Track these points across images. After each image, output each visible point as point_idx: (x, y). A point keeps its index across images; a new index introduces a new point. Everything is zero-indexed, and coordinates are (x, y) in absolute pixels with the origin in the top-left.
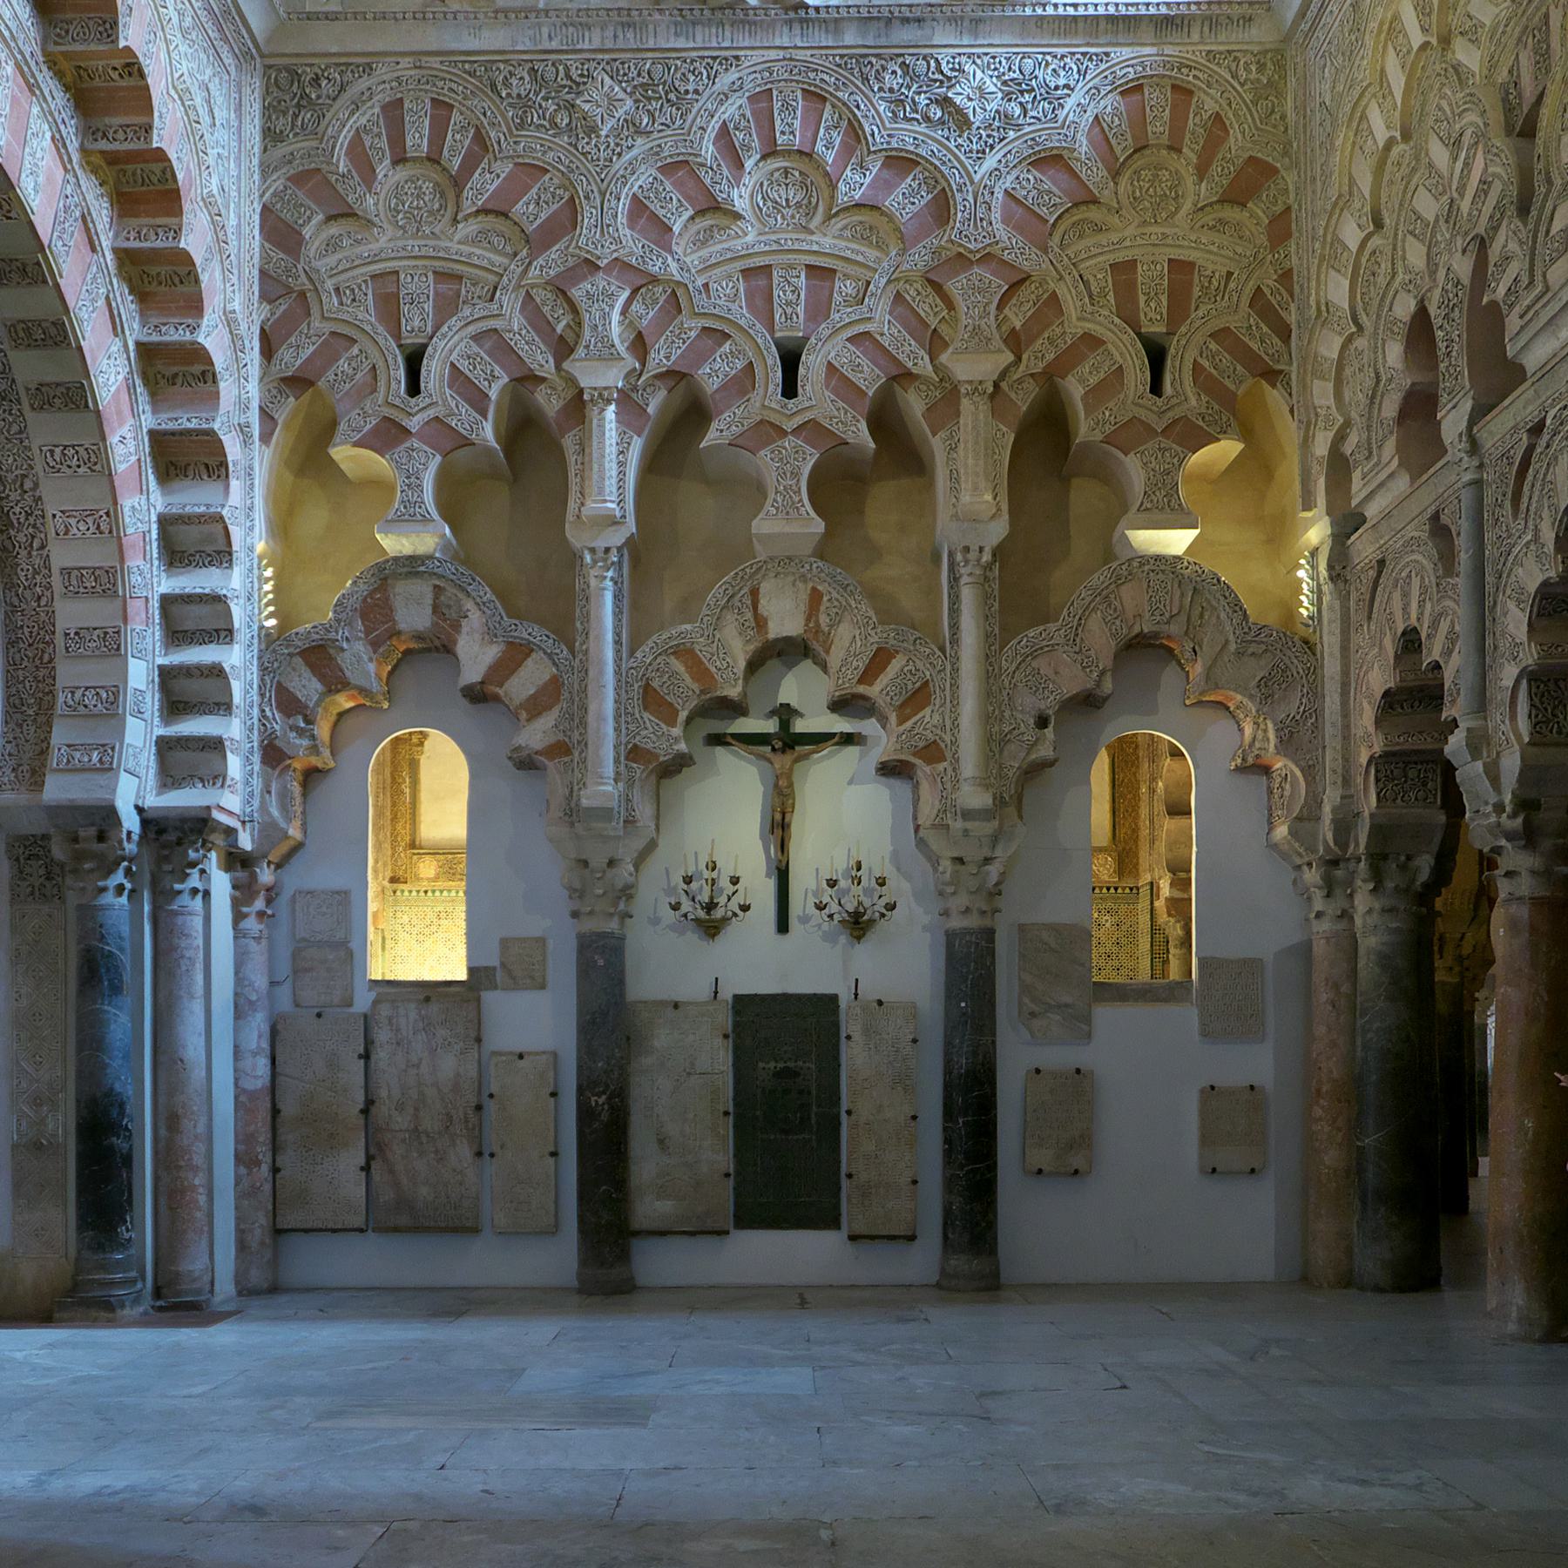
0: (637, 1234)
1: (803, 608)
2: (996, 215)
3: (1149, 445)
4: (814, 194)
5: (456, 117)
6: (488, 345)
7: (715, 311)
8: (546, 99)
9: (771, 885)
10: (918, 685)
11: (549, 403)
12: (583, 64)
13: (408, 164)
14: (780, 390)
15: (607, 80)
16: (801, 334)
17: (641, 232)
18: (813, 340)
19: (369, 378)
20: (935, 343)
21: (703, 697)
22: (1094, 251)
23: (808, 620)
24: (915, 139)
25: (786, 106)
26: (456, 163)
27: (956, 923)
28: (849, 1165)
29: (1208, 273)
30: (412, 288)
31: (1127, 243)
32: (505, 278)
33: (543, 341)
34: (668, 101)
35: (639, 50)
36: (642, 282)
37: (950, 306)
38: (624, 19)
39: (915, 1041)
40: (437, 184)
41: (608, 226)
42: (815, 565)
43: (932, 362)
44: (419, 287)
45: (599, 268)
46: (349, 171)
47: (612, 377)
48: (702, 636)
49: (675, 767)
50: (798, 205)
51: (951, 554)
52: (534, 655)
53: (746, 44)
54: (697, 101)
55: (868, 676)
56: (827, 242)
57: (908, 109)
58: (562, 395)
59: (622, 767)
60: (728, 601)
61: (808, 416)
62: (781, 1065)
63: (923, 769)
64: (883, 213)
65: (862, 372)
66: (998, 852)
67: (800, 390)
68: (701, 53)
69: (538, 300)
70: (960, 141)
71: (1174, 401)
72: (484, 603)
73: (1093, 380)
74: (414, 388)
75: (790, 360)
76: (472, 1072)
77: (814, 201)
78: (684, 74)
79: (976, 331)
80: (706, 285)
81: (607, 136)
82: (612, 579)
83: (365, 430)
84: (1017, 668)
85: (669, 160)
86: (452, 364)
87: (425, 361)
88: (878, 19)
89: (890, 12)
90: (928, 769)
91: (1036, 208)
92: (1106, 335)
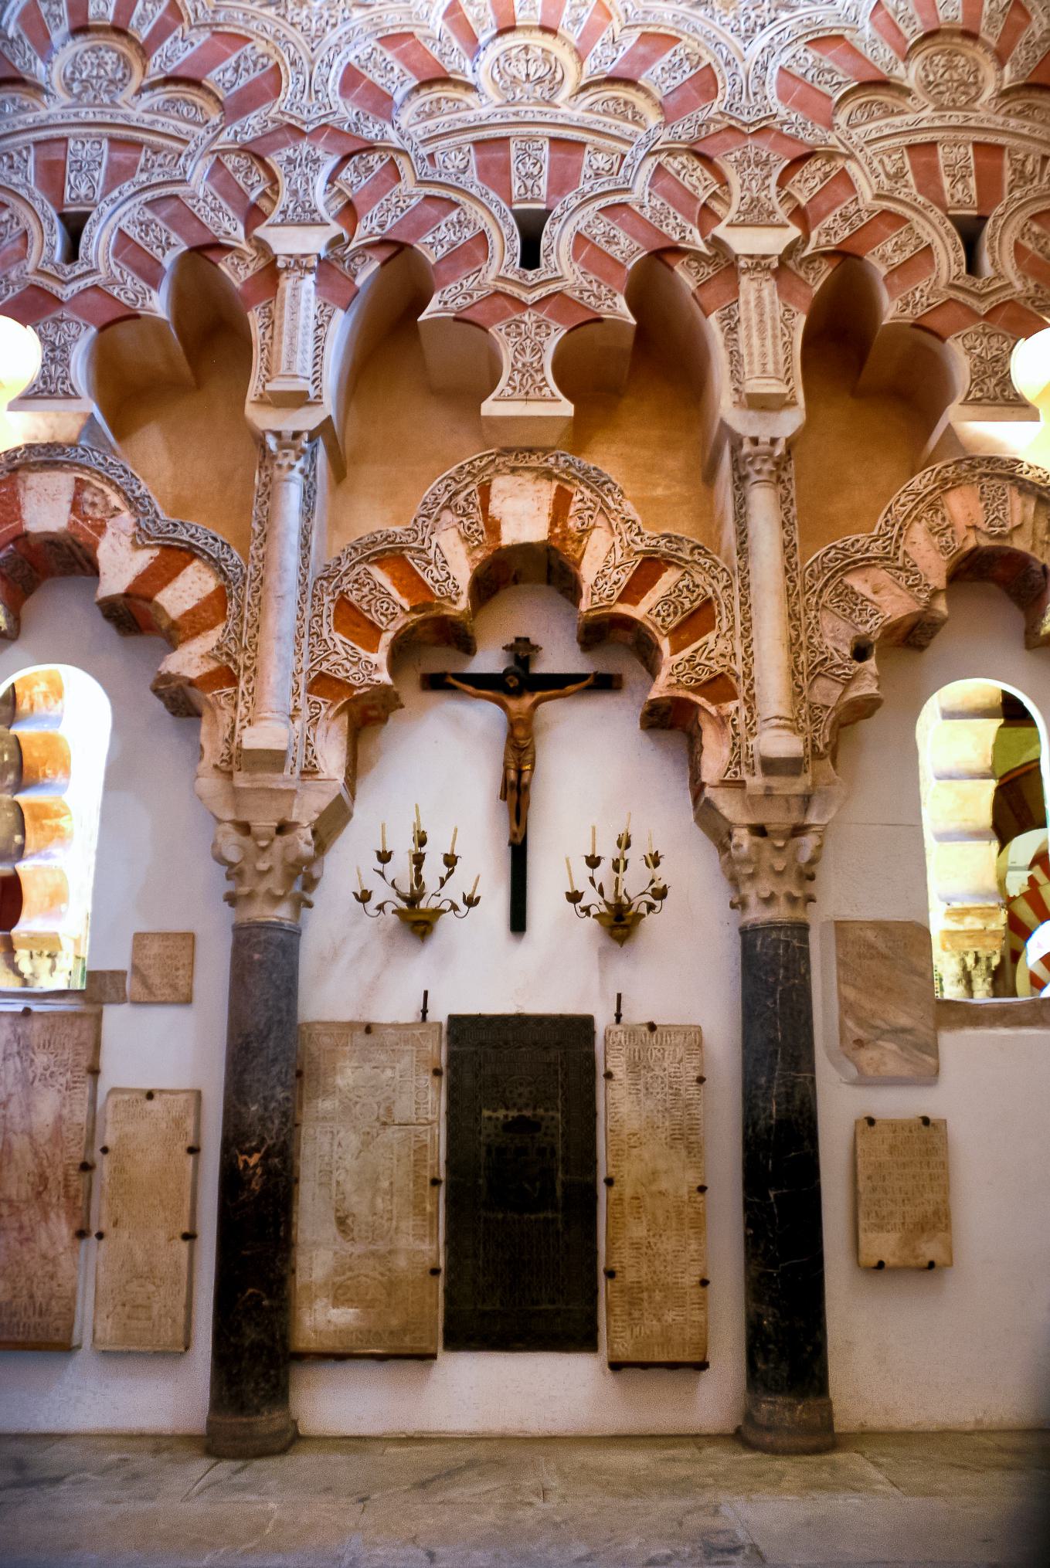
0: (302, 1357)
1: (547, 509)
2: (771, 90)
3: (971, 328)
4: (559, 70)
6: (164, 214)
7: (443, 179)
10: (697, 604)
11: (236, 273)
13: (90, 36)
14: (518, 260)
16: (543, 206)
17: (359, 100)
18: (558, 210)
19: (18, 245)
21: (415, 616)
22: (887, 132)
23: (553, 523)
24: (674, 16)
26: (144, 33)
28: (608, 1258)
29: (1020, 156)
30: (81, 155)
31: (924, 124)
32: (192, 146)
33: (233, 208)
37: (724, 182)
39: (701, 1080)
40: (121, 56)
41: (317, 92)
42: (562, 459)
43: (703, 235)
45: (303, 134)
46: (19, 36)
47: (313, 242)
48: (415, 540)
50: (540, 80)
51: (733, 451)
52: (196, 563)
55: (634, 591)
56: (571, 109)
58: (252, 266)
59: (302, 703)
60: (450, 499)
61: (553, 288)
62: (514, 1113)
64: (640, 88)
65: (618, 244)
66: (812, 819)
67: (543, 261)
69: (230, 167)
70: (725, 20)
71: (998, 284)
72: (137, 499)
73: (898, 259)
74: (72, 253)
76: (81, 1116)
77: (558, 76)
79: (755, 202)
80: (431, 156)
81: (320, 8)
82: (302, 471)
83: (7, 298)
84: (825, 585)
85: (391, 32)
86: (121, 231)
87: (87, 227)
90: (712, 710)
91: (816, 85)
92: (908, 213)
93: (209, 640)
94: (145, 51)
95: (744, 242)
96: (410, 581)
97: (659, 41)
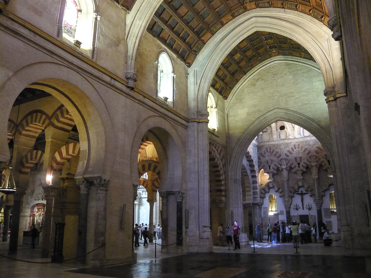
2: (314, 152)
5: (271, 149)
9: (302, 206)
17: (286, 156)
20: (310, 162)
26: (272, 152)
27: (318, 208)
36: (286, 159)
44: (270, 161)
47: (285, 167)
49: (292, 197)
56: (301, 155)
63: (313, 196)
74: (270, 169)
75: (299, 164)
93: (282, 193)
94: (272, 153)
95: (313, 164)
96: (294, 189)
97: (306, 149)
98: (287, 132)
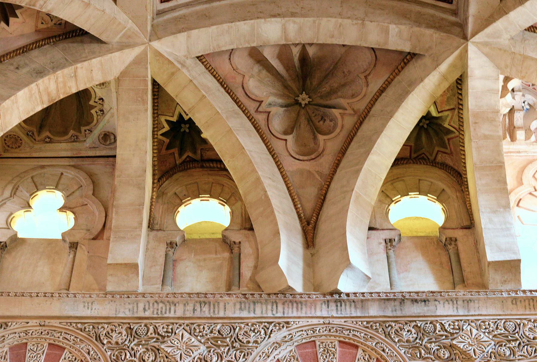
8: (138, 345)
12: (168, 326)
15: (186, 335)
25: (326, 350)
34: (233, 347)
35: (211, 318)
38: (202, 299)
53: (295, 314)
54: (257, 348)
57: (423, 352)
68: (259, 320)
78: (246, 332)
88: (395, 300)
89: (402, 296)
98: (247, 250)
